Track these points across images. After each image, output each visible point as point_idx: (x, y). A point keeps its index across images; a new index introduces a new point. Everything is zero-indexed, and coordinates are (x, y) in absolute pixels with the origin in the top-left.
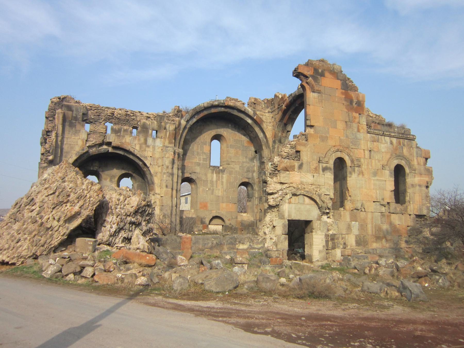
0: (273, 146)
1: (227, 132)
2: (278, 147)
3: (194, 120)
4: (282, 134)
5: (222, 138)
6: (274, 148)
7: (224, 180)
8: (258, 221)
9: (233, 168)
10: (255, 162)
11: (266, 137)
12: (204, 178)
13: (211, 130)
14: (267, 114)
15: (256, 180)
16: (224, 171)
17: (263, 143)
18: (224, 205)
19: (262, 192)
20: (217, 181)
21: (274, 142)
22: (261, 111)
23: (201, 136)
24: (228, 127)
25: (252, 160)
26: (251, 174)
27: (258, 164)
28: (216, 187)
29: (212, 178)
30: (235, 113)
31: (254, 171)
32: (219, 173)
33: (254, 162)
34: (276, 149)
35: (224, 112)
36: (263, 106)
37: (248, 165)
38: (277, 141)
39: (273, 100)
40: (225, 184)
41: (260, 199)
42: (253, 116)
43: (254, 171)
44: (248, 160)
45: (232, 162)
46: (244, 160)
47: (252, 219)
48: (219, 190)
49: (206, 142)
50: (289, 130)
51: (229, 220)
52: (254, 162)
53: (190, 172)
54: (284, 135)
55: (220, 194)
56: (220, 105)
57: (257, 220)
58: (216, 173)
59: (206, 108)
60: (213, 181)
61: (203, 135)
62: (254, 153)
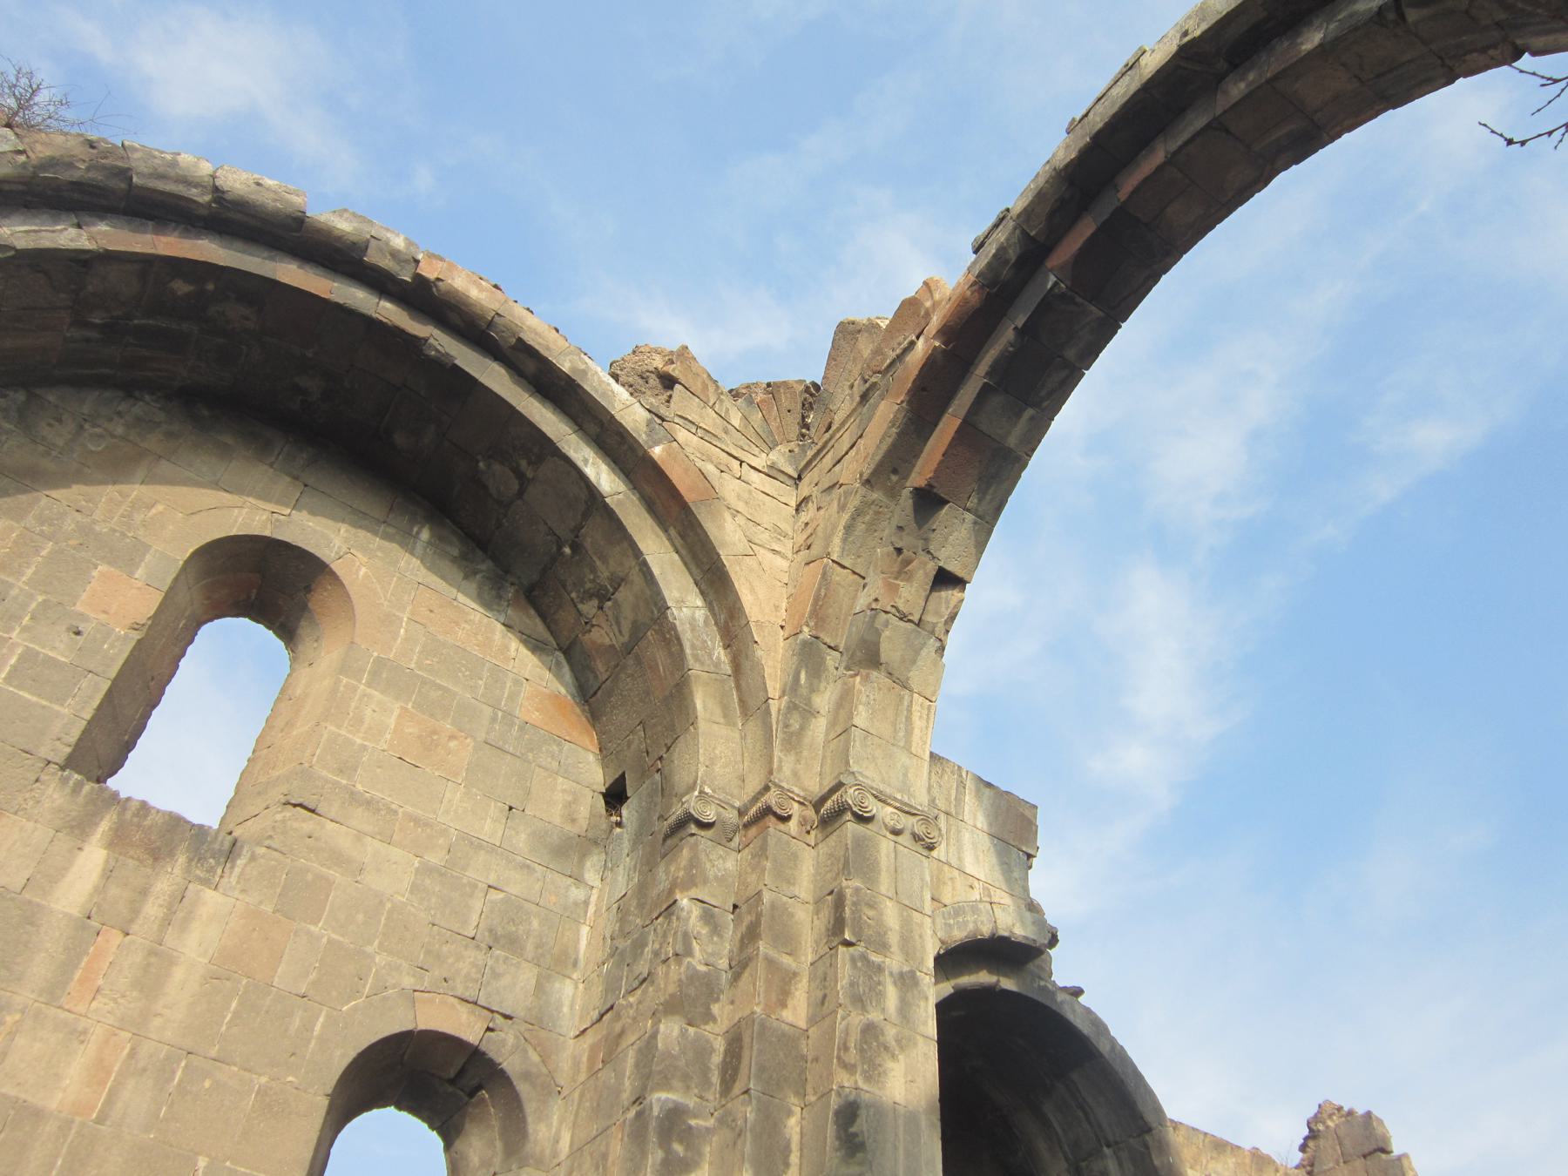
0: (792, 688)
1: (386, 578)
2: (845, 701)
3: (66, 236)
4: (893, 589)
5: (320, 599)
6: (801, 708)
7: (196, 945)
9: (338, 859)
10: (592, 877)
13: (239, 490)
14: (754, 476)
15: (571, 1053)
17: (696, 670)
20: (88, 924)
21: (809, 655)
22: (707, 435)
23: (111, 490)
24: (406, 540)
25: (569, 851)
26: (527, 976)
28: (53, 992)
29: (49, 874)
30: (495, 378)
31: (563, 962)
32: (158, 853)
33: (578, 879)
34: (819, 726)
35: (398, 332)
36: (736, 420)
37: (517, 884)
38: (832, 659)
39: (813, 395)
40: (182, 984)
42: (642, 438)
43: (563, 962)
44: (521, 840)
45: (354, 798)
46: (490, 827)
49: (147, 548)
50: (954, 567)
52: (578, 879)
56: (373, 257)
58: (118, 840)
59: (231, 217)
60: (31, 916)
61: (136, 491)
62: (591, 804)
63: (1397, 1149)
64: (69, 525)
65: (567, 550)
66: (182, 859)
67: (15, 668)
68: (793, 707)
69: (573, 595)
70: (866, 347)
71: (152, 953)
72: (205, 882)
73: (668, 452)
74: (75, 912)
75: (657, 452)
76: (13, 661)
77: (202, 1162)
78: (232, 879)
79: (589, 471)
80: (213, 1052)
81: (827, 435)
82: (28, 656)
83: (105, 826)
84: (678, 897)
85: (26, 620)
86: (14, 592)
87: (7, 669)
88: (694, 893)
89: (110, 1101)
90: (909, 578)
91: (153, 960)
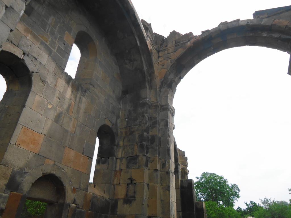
0: (160, 88)
8: (120, 203)
11: (151, 74)
12: (50, 79)
16: (85, 92)
18: (72, 154)
19: (136, 148)
21: (162, 83)
26: (115, 118)
27: (129, 107)
29: (65, 91)
32: (77, 90)
41: (132, 160)
47: (106, 196)
48: (71, 119)
51: (74, 190)
52: (120, 104)
53: (27, 50)
54: (177, 79)
55: (70, 128)
57: (116, 201)
60: (64, 97)
63: (186, 156)
64: (61, 21)
65: (127, 51)
66: (80, 92)
67: (57, 49)
68: (160, 90)
69: (125, 58)
70: (177, 38)
71: (78, 107)
72: (83, 96)
73: (148, 42)
74: (69, 98)
75: (147, 42)
76: (57, 48)
77: (85, 141)
78: (85, 96)
79: (137, 41)
80: (85, 124)
81: (166, 48)
82: (59, 47)
83: (71, 83)
84: (145, 115)
85: (58, 40)
86: (56, 33)
87: (56, 49)
88: (147, 115)
89: (75, 130)
90: (177, 77)
91: (78, 108)
